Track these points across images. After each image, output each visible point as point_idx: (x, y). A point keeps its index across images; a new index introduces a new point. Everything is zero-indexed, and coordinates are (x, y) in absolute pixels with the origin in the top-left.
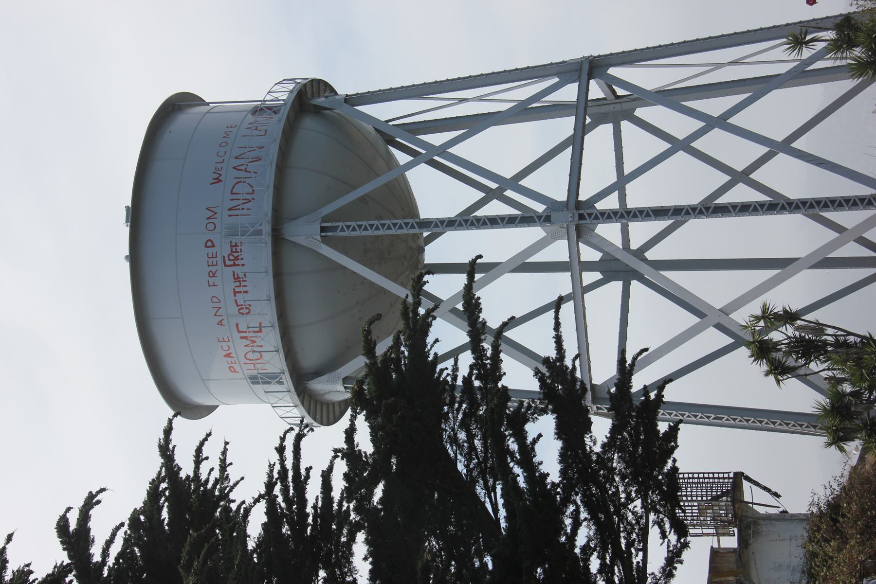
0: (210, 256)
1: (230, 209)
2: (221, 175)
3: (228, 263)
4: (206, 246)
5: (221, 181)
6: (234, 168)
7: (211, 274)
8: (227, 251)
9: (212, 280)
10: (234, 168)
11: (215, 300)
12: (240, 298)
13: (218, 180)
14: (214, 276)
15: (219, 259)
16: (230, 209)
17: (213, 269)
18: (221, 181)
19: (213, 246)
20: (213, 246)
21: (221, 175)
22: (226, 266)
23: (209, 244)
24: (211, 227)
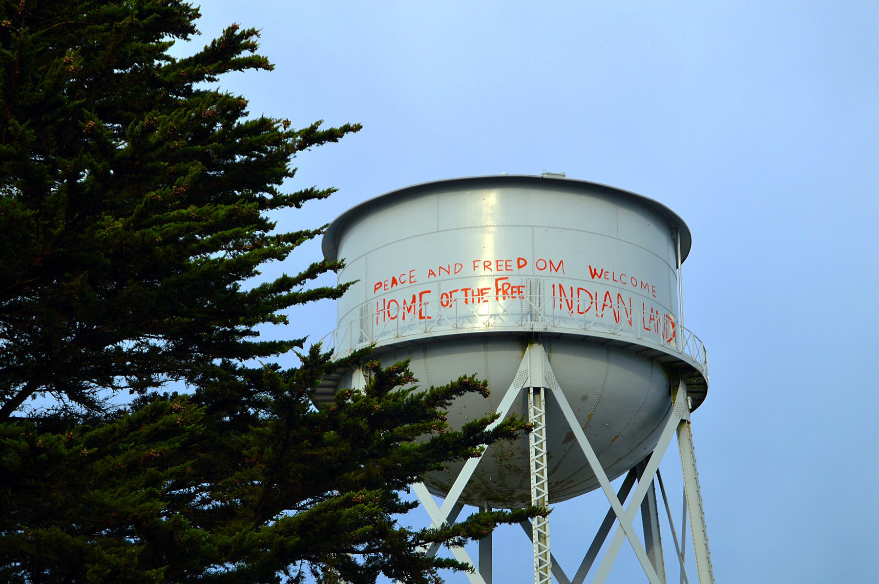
1: (561, 286)
4: (519, 259)
5: (593, 277)
6: (608, 293)
7: (487, 264)
8: (514, 281)
10: (608, 293)
12: (460, 295)
14: (485, 267)
15: (504, 273)
16: (561, 286)
17: (493, 266)
18: (593, 277)
19: (519, 267)
20: (519, 267)
22: (497, 280)
23: (522, 263)
24: (541, 265)
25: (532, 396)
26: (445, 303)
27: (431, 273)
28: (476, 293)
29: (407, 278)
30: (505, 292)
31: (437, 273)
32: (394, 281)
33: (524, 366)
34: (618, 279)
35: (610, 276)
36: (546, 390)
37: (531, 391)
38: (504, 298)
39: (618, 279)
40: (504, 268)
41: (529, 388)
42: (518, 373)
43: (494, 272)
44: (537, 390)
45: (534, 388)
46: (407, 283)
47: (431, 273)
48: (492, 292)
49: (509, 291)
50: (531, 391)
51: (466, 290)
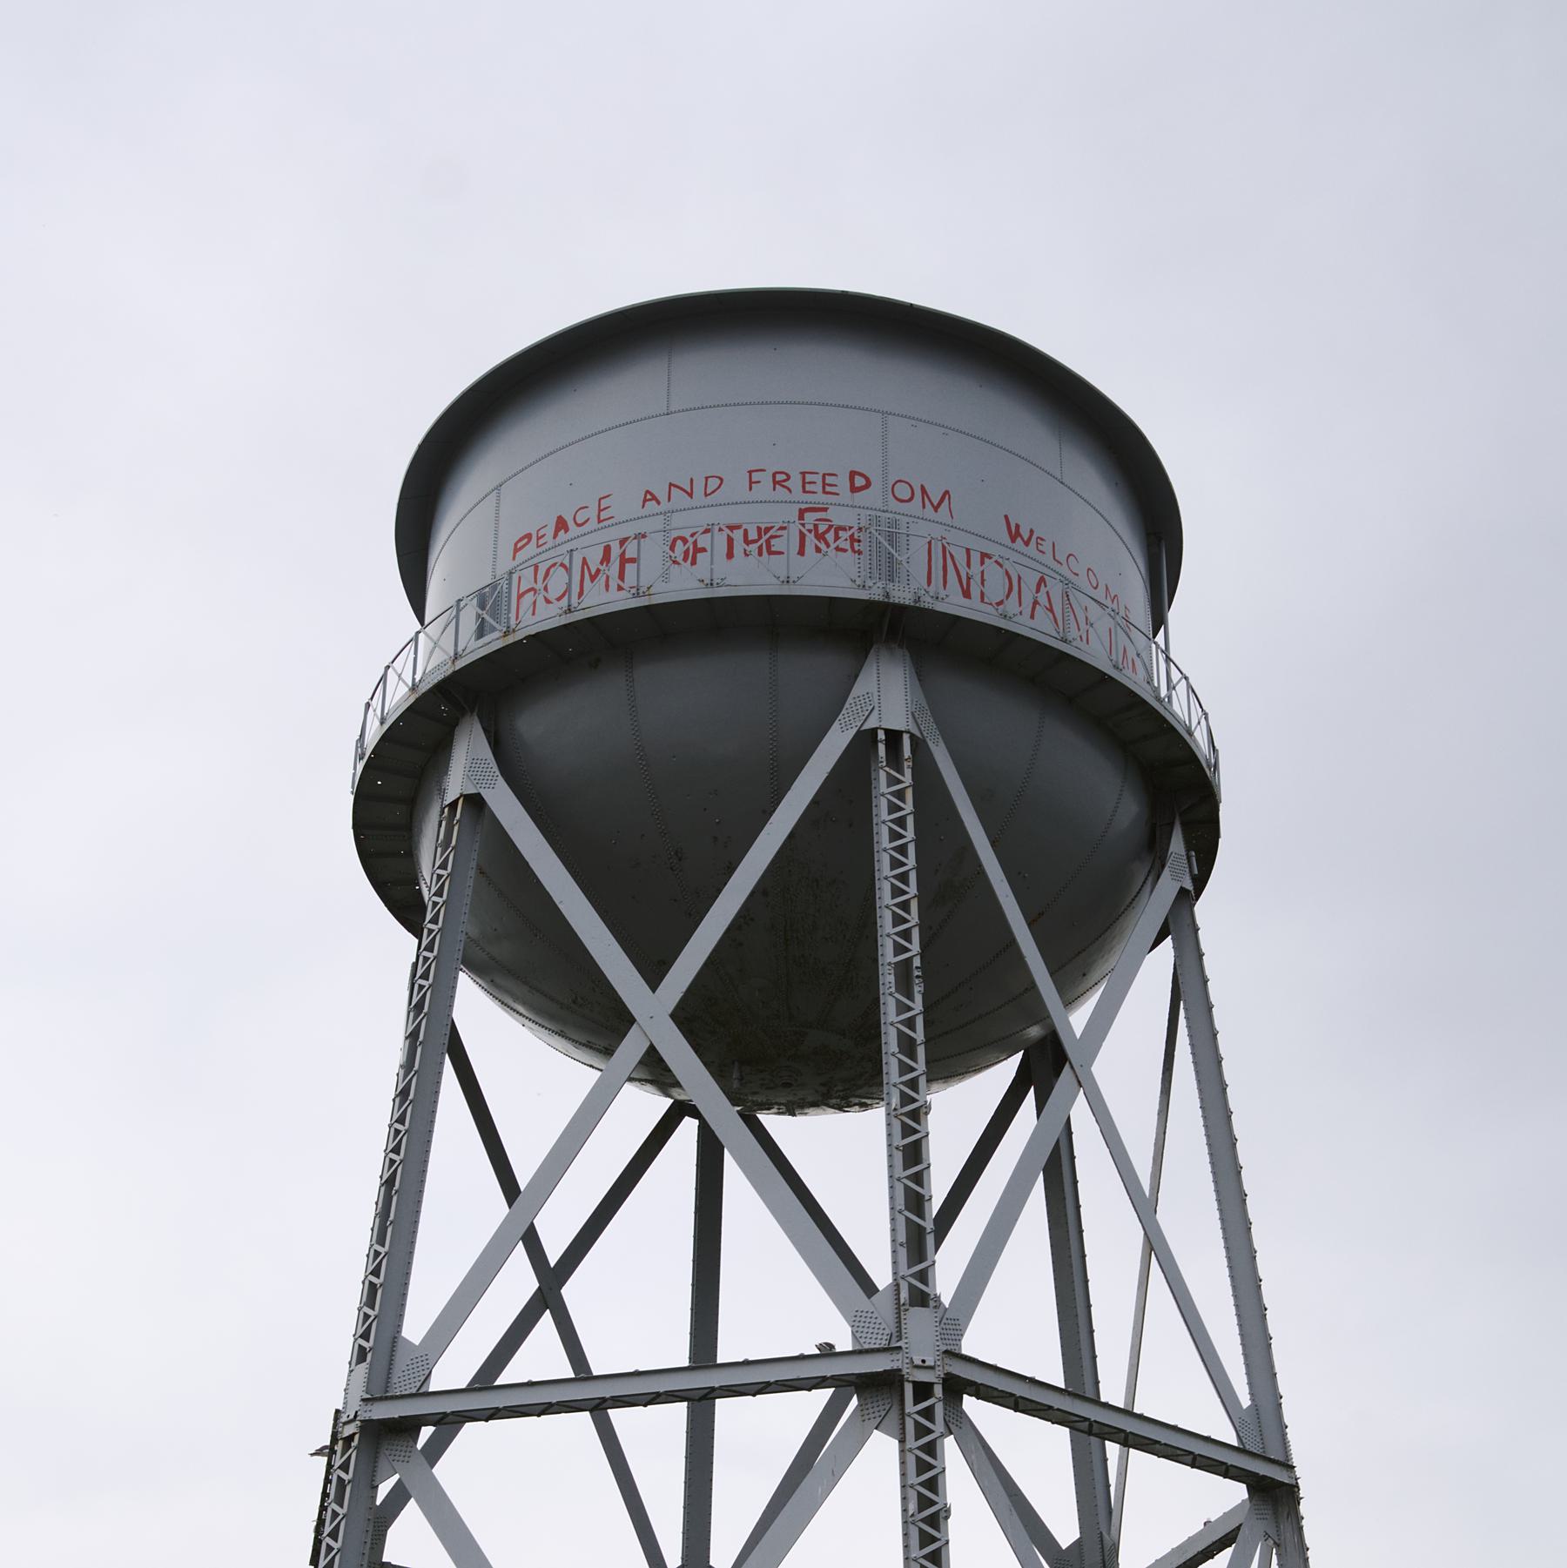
0: (829, 480)
2: (1027, 543)
3: (810, 518)
4: (853, 474)
5: (1013, 541)
7: (780, 477)
9: (766, 479)
11: (713, 483)
13: (1015, 534)
14: (775, 483)
15: (820, 498)
18: (1013, 541)
19: (854, 489)
20: (854, 489)
21: (1027, 543)
23: (859, 482)
25: (882, 748)
26: (679, 543)
27: (649, 497)
28: (753, 535)
29: (592, 513)
30: (820, 537)
31: (662, 497)
32: (561, 524)
33: (865, 685)
34: (1063, 560)
35: (1046, 546)
36: (912, 736)
37: (881, 735)
38: (818, 550)
39: (1063, 560)
40: (818, 487)
41: (874, 731)
42: (850, 700)
43: (797, 494)
44: (894, 737)
45: (887, 731)
46: (593, 524)
47: (649, 497)
48: (794, 530)
49: (830, 537)
50: (881, 735)
51: (732, 528)
